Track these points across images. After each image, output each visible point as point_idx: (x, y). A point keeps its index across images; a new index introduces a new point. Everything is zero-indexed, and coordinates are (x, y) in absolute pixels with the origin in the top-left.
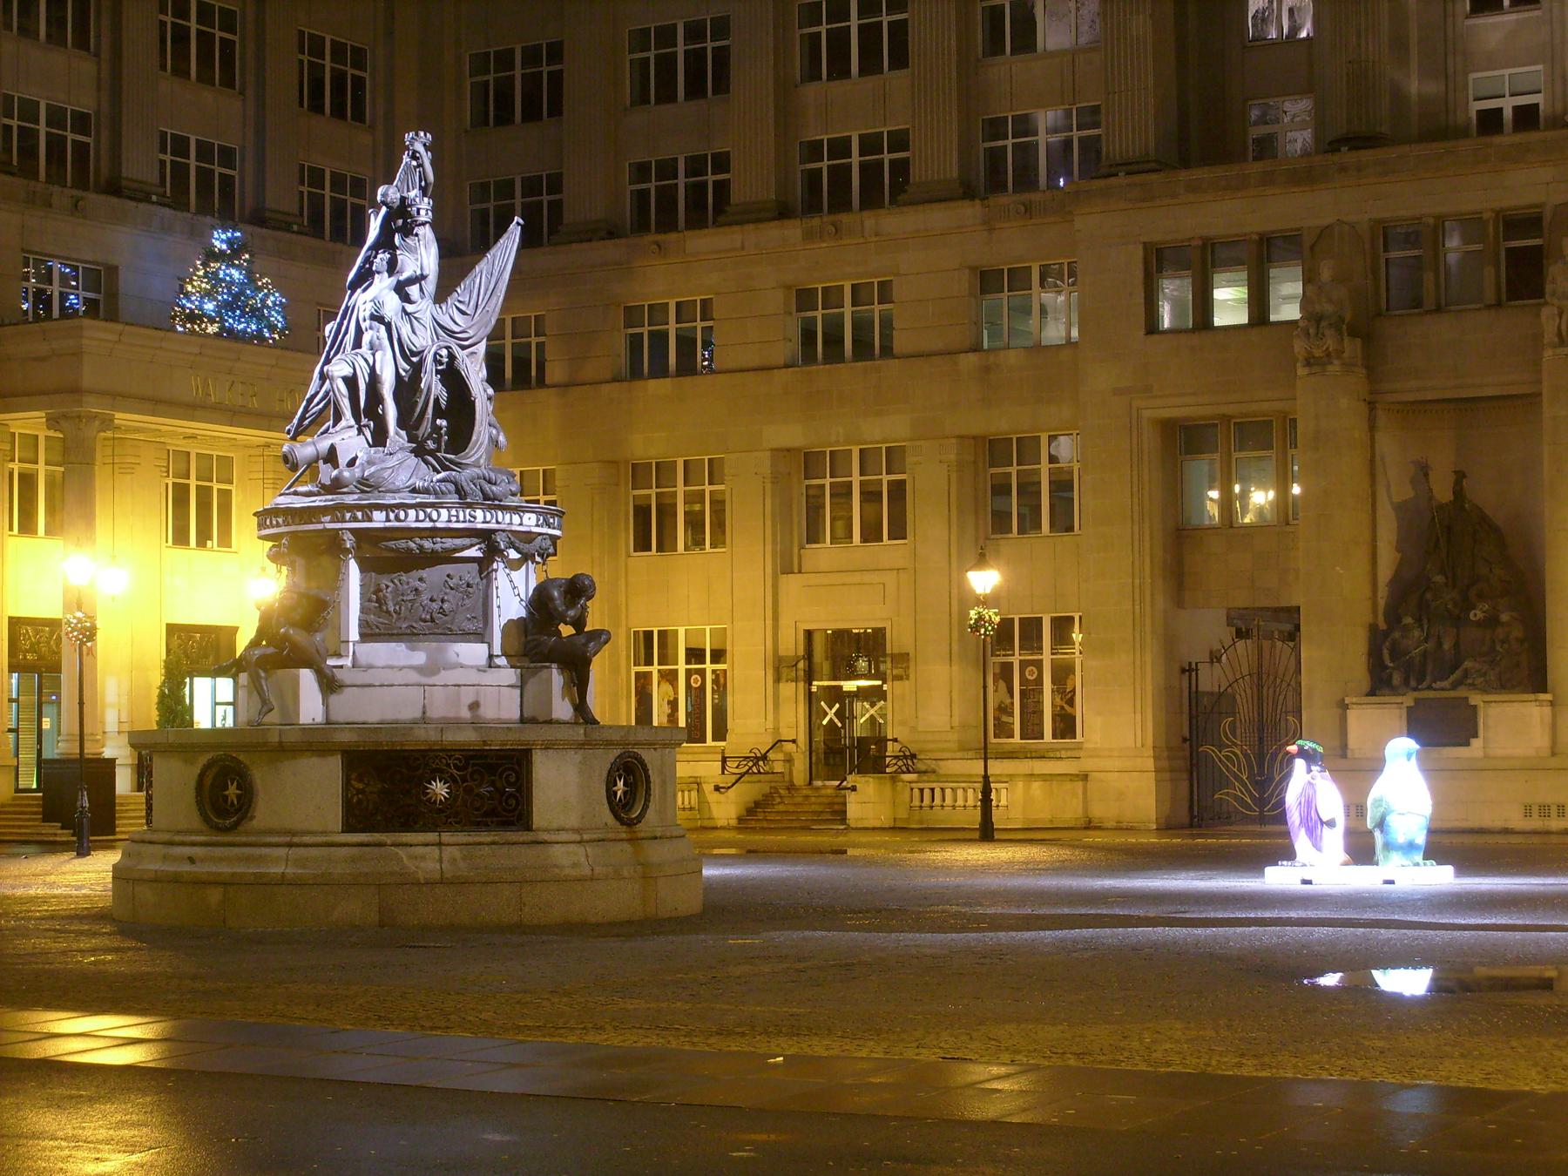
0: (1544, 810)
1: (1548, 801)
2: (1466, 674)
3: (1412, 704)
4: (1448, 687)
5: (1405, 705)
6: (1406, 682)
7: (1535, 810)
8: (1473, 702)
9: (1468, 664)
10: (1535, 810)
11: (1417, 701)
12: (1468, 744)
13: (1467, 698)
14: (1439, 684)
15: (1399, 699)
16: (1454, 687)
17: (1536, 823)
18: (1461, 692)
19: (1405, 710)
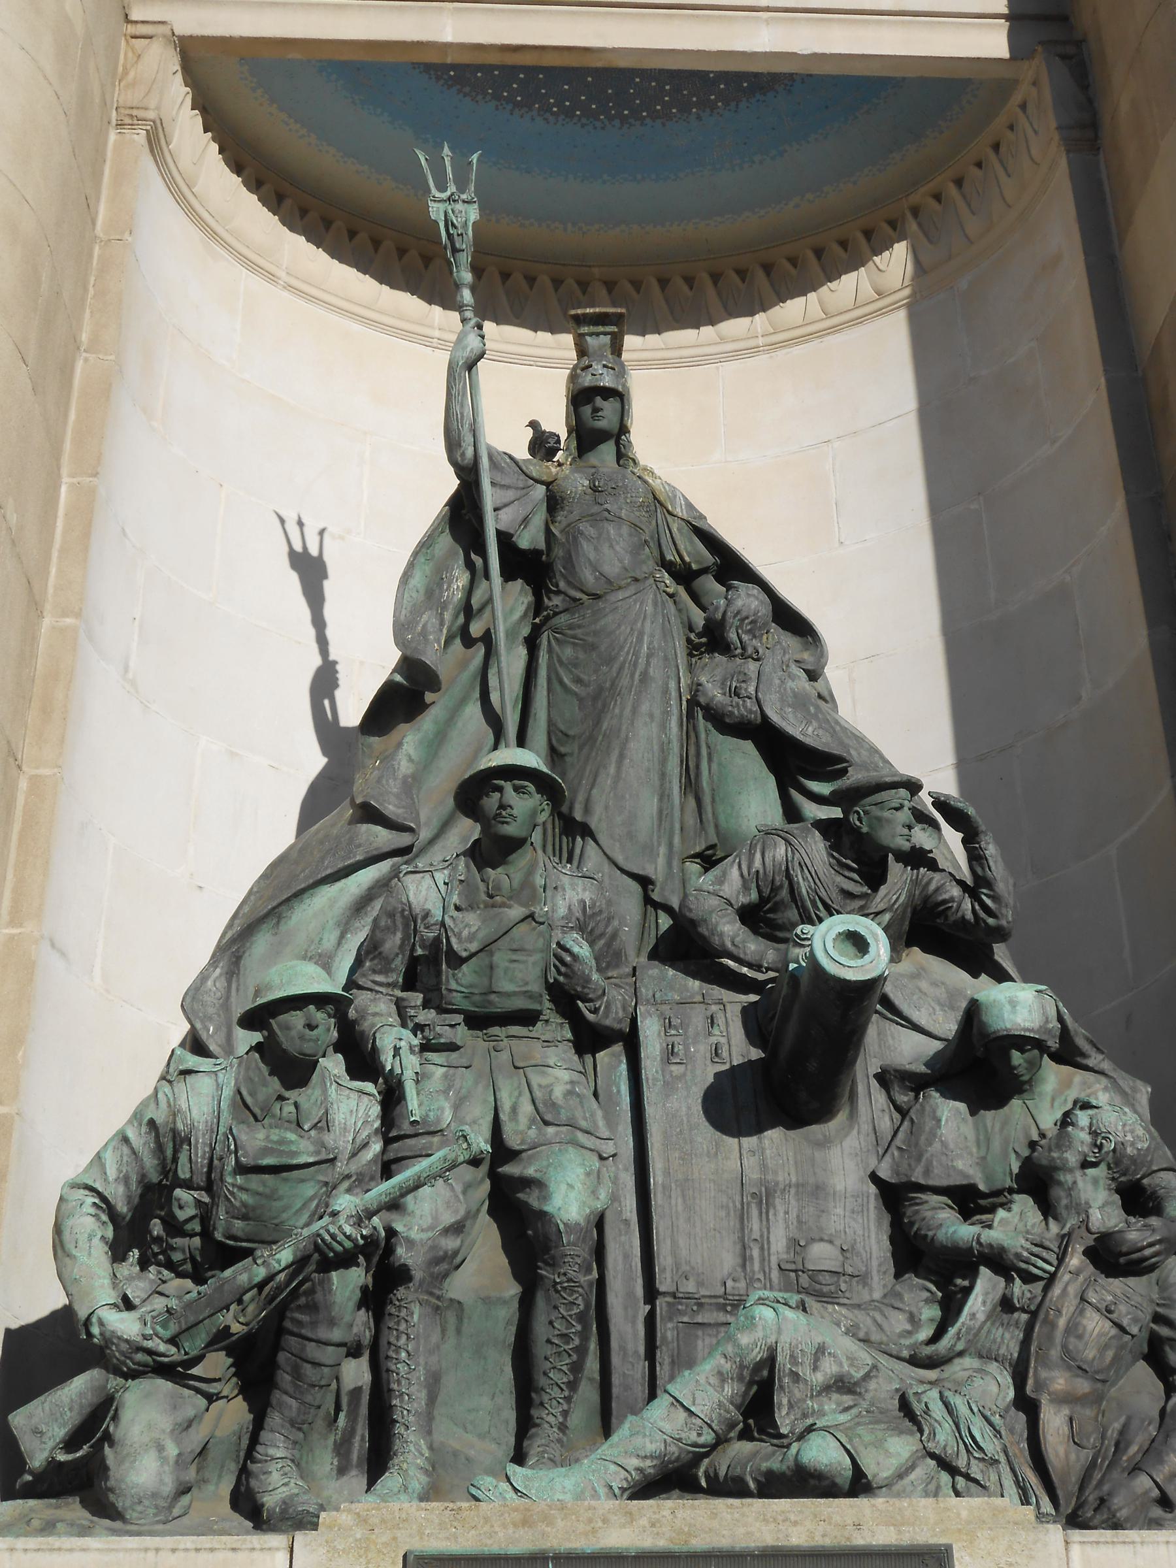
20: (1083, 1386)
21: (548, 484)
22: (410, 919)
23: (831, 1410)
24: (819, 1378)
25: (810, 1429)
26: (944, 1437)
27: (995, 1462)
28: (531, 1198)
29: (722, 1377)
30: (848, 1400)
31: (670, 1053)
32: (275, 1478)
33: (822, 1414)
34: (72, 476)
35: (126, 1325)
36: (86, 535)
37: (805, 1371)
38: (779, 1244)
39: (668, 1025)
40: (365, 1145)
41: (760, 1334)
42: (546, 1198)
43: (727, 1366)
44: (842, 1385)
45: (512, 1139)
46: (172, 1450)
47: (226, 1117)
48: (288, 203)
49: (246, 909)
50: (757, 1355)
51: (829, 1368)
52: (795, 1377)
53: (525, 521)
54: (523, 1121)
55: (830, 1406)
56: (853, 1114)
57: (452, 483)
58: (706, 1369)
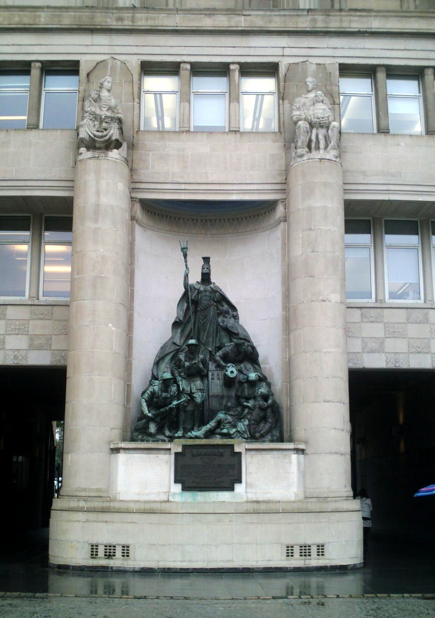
0: (305, 550)
1: (309, 542)
2: (219, 423)
3: (180, 450)
4: (202, 436)
5: (173, 452)
6: (160, 430)
7: (297, 550)
8: (237, 450)
9: (221, 416)
10: (297, 550)
11: (185, 447)
12: (232, 489)
13: (232, 446)
14: (194, 433)
15: (168, 446)
16: (210, 434)
17: (297, 562)
18: (217, 440)
19: (173, 457)
20: (256, 423)
21: (198, 290)
22: (180, 360)
23: (227, 426)
24: (226, 422)
25: (224, 428)
26: (239, 429)
27: (244, 432)
28: (195, 399)
29: (215, 422)
30: (229, 424)
31: (213, 379)
32: (167, 432)
33: (226, 426)
34: (130, 287)
35: (150, 415)
36: (133, 298)
37: (224, 422)
38: (224, 403)
39: (213, 375)
40: (175, 393)
41: (219, 418)
42: (196, 399)
43: (216, 421)
44: (229, 423)
45: (193, 391)
46: (155, 429)
47: (160, 392)
48: (156, 214)
49: (158, 355)
50: (219, 420)
51: (227, 421)
52: (223, 422)
53: (195, 296)
54: (194, 389)
55: (227, 425)
56: (234, 386)
57: (184, 290)
58: (213, 421)
